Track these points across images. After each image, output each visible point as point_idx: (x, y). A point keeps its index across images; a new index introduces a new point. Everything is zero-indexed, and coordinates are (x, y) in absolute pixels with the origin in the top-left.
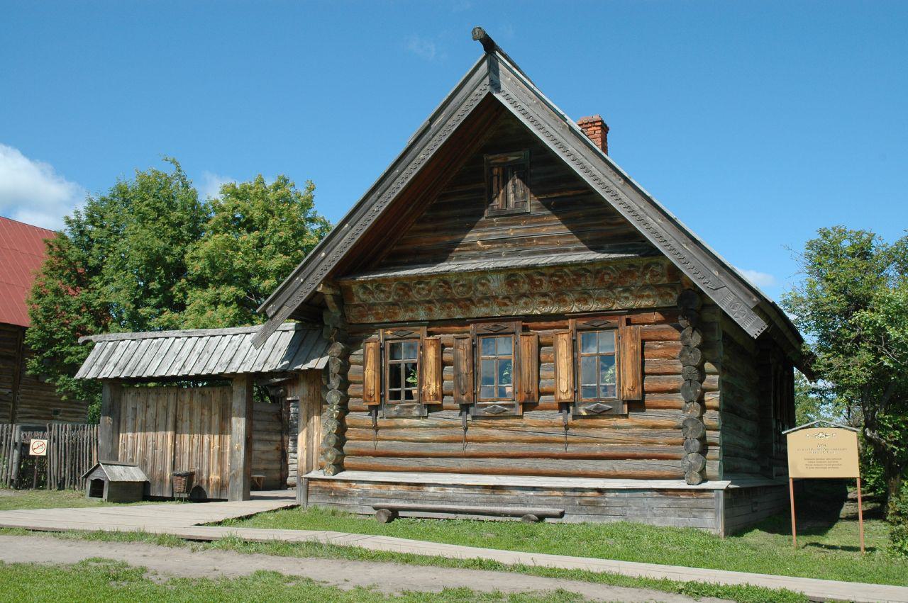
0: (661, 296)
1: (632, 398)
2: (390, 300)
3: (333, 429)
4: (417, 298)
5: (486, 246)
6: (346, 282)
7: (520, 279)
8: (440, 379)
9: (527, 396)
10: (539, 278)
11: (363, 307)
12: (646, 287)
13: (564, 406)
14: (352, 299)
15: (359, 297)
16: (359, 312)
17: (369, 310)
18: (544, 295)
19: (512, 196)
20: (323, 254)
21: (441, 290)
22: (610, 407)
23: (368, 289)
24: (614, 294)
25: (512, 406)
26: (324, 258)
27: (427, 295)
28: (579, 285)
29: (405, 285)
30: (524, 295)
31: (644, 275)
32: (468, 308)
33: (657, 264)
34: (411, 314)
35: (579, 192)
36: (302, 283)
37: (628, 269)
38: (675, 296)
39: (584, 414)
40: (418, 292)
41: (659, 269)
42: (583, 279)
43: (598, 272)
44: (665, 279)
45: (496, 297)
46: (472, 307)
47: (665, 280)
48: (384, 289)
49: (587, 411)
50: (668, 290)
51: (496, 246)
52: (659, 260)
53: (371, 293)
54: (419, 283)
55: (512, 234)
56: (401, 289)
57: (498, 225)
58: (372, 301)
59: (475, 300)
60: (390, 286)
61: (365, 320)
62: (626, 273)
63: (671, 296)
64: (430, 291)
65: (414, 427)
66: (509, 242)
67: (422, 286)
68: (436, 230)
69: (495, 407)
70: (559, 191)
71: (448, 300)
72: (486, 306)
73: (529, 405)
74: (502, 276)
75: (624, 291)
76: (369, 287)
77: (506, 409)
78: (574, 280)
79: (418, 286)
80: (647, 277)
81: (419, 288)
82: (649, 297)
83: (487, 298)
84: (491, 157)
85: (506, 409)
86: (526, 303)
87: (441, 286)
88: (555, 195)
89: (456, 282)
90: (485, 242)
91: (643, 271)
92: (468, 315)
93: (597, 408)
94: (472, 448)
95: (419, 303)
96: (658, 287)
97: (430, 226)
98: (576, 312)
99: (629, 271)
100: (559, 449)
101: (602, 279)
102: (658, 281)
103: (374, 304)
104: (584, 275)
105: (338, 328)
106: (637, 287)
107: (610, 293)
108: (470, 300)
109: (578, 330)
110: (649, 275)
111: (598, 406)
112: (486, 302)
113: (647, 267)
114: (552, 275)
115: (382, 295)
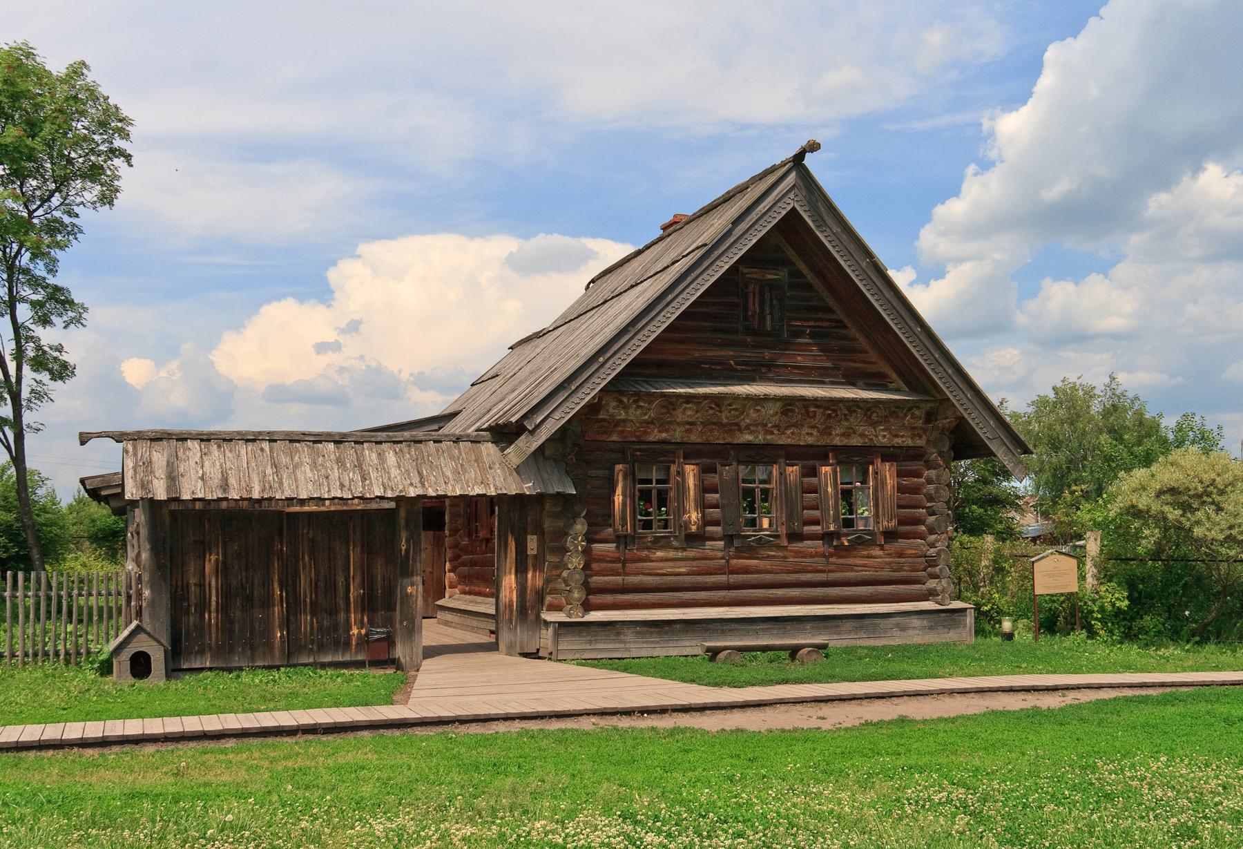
0: (913, 437)
8: (703, 505)
12: (904, 427)
13: (828, 537)
17: (616, 426)
18: (814, 427)
19: (768, 318)
21: (711, 412)
23: (621, 402)
27: (691, 416)
28: (847, 420)
29: (671, 403)
30: (794, 425)
31: (906, 415)
32: (731, 432)
34: (664, 435)
38: (924, 437)
41: (917, 413)
43: (868, 409)
46: (738, 433)
47: (920, 423)
50: (921, 432)
53: (626, 408)
54: (688, 402)
56: (663, 407)
58: (623, 415)
59: (743, 424)
60: (650, 403)
61: (604, 437)
62: (892, 414)
63: (921, 437)
65: (667, 562)
66: (763, 366)
68: (681, 342)
70: (815, 320)
72: (751, 433)
73: (795, 537)
74: (778, 404)
76: (625, 400)
83: (756, 425)
84: (746, 270)
88: (811, 323)
92: (729, 440)
94: (734, 578)
95: (679, 424)
96: (913, 428)
101: (870, 417)
103: (624, 421)
108: (737, 425)
114: (828, 408)
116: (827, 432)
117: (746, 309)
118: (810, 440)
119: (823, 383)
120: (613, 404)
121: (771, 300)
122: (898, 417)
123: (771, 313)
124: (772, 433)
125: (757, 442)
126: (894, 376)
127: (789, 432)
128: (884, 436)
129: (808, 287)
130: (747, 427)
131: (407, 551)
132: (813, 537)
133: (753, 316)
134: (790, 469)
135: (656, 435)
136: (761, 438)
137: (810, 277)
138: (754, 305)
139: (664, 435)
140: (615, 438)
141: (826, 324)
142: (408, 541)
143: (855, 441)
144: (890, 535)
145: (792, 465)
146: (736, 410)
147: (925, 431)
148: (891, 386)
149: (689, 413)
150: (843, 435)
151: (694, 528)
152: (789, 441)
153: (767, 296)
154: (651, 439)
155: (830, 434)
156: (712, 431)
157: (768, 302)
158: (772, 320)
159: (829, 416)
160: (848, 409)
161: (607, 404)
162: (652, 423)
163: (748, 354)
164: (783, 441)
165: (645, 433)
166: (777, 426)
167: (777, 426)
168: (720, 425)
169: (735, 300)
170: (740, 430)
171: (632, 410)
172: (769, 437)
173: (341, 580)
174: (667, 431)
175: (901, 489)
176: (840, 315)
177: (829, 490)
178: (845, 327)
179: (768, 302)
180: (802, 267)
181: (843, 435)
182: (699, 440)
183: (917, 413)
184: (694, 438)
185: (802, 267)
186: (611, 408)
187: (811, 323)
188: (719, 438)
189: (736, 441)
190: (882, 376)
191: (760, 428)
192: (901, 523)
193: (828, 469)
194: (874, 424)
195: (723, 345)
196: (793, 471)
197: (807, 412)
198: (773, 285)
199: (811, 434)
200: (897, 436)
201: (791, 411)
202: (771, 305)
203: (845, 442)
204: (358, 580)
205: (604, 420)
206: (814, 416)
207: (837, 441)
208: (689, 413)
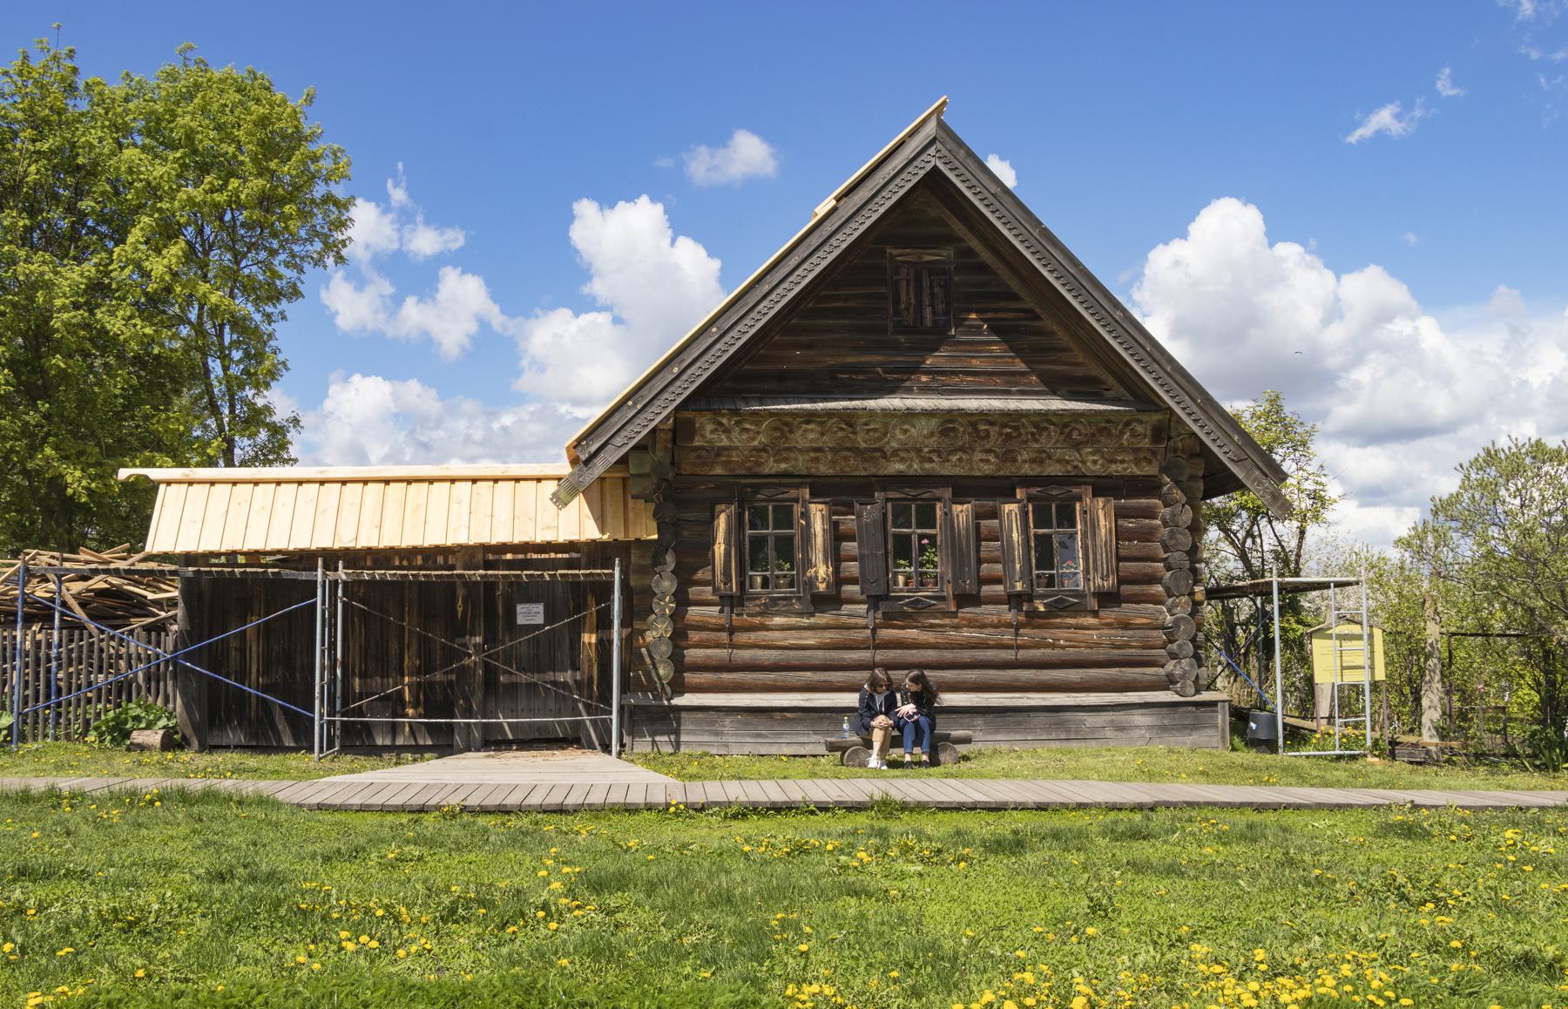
2: (756, 443)
4: (802, 444)
6: (690, 415)
12: (1122, 449)
13: (1014, 600)
14: (691, 439)
15: (703, 436)
16: (699, 457)
19: (928, 310)
21: (840, 434)
23: (720, 424)
25: (942, 599)
28: (1037, 441)
29: (786, 424)
30: (961, 449)
31: (1122, 433)
34: (783, 466)
40: (804, 436)
41: (1139, 429)
43: (1066, 425)
45: (919, 451)
47: (1146, 443)
50: (1149, 456)
53: (727, 431)
54: (808, 422)
56: (776, 429)
58: (725, 442)
60: (758, 424)
61: (705, 470)
62: (1102, 431)
63: (1150, 462)
64: (822, 434)
68: (810, 346)
70: (996, 311)
71: (848, 449)
72: (902, 460)
74: (934, 422)
75: (1093, 454)
76: (724, 421)
78: (1033, 434)
79: (805, 426)
82: (1122, 462)
83: (907, 451)
84: (895, 252)
86: (960, 460)
89: (866, 424)
92: (872, 471)
97: (803, 339)
100: (1008, 655)
101: (1069, 436)
112: (902, 454)
113: (1127, 424)
114: (1005, 426)
115: (745, 436)
116: (1008, 457)
117: (897, 301)
118: (987, 469)
119: (1008, 393)
120: (710, 427)
121: (931, 288)
122: (1110, 435)
123: (932, 305)
124: (931, 461)
125: (911, 472)
126: (1111, 381)
127: (954, 458)
128: (1095, 462)
129: (983, 268)
130: (895, 452)
131: (465, 613)
132: (994, 600)
133: (907, 309)
134: (957, 508)
135: (772, 466)
136: (916, 467)
137: (985, 256)
138: (906, 296)
139: (783, 466)
140: (719, 471)
141: (1012, 315)
142: (465, 602)
143: (1053, 469)
144: (1108, 599)
145: (962, 503)
146: (875, 430)
148: (1108, 394)
149: (811, 436)
150: (1033, 461)
151: (822, 587)
152: (958, 471)
153: (926, 283)
154: (766, 471)
155: (1015, 460)
156: (846, 459)
157: (926, 291)
158: (934, 313)
159: (1008, 435)
160: (1036, 425)
161: (702, 427)
162: (764, 450)
164: (946, 470)
165: (759, 464)
166: (938, 452)
167: (938, 452)
168: (858, 452)
169: (883, 290)
170: (885, 456)
171: (735, 434)
172: (927, 466)
173: (394, 646)
174: (786, 460)
175: (1121, 534)
176: (1029, 303)
177: (1015, 535)
178: (1038, 318)
179: (926, 291)
180: (974, 244)
181: (1033, 461)
182: (831, 472)
183: (1139, 429)
184: (823, 469)
185: (974, 244)
186: (708, 432)
188: (857, 468)
189: (882, 472)
190: (1094, 381)
191: (913, 454)
192: (1121, 581)
193: (1014, 507)
194: (1077, 446)
195: (866, 350)
196: (962, 512)
197: (977, 431)
198: (934, 269)
199: (988, 461)
200: (1113, 461)
201: (953, 430)
202: (932, 295)
204: (414, 647)
205: (702, 448)
206: (988, 436)
207: (1027, 470)
208: (811, 436)
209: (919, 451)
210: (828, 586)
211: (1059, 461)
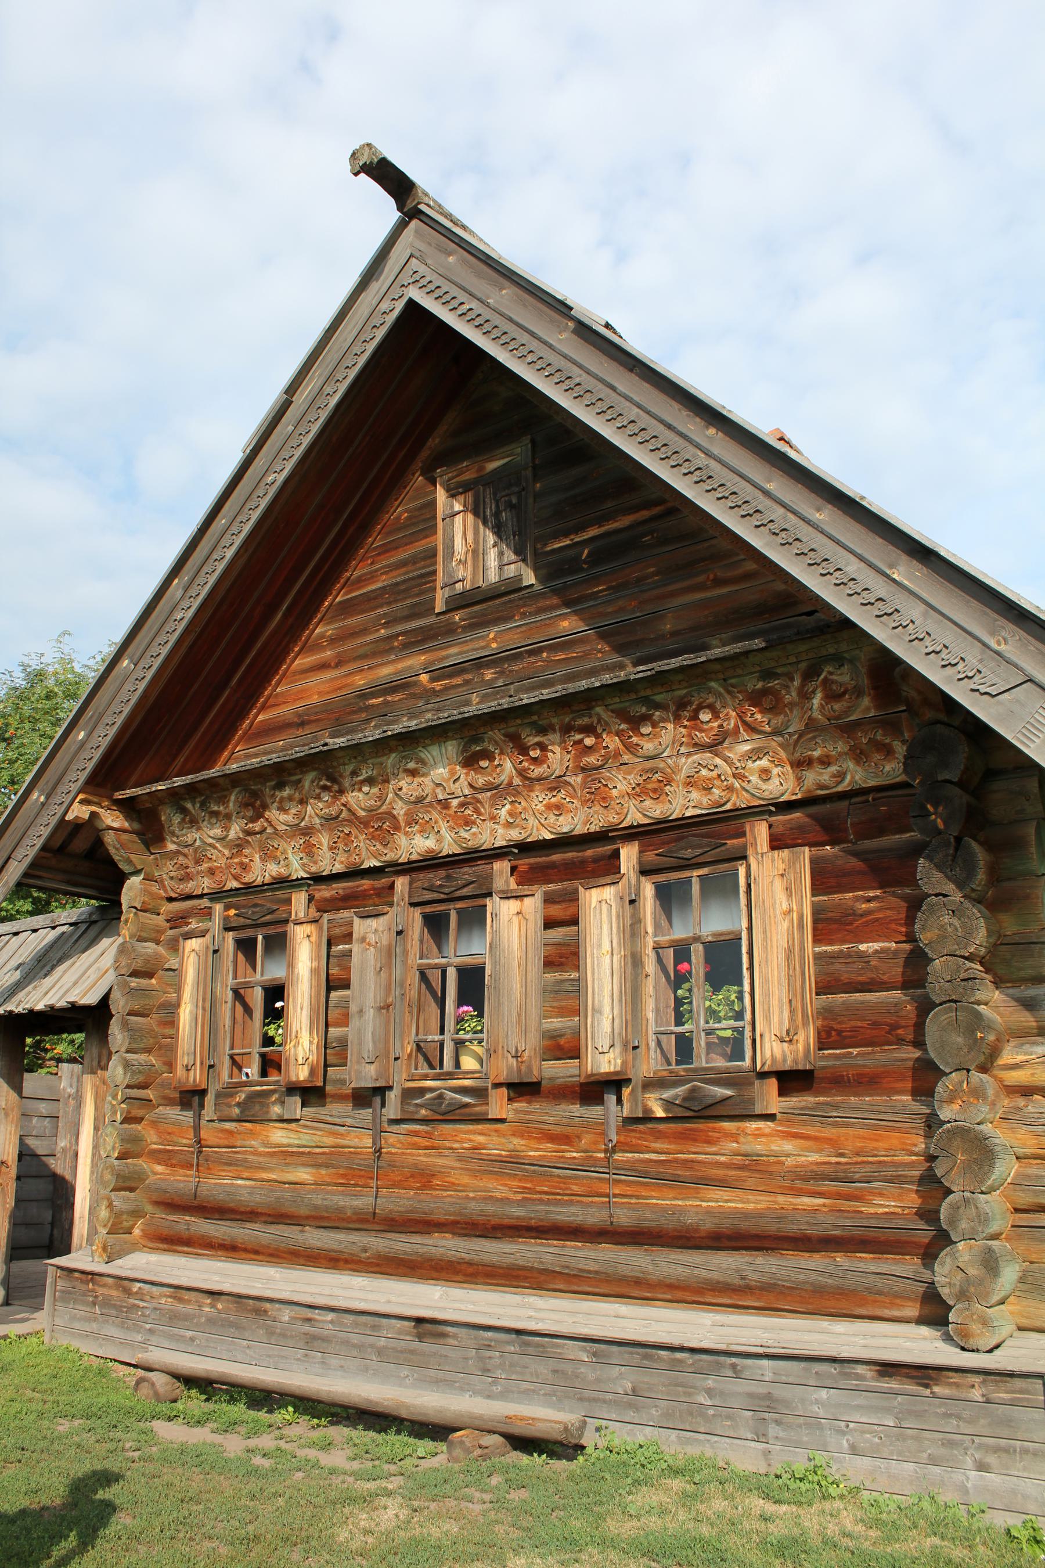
0: (859, 755)
1: (788, 1065)
3: (114, 1148)
5: (438, 686)
7: (491, 748)
9: (513, 1062)
10: (537, 739)
11: (185, 855)
17: (198, 862)
18: (556, 784)
20: (82, 735)
22: (729, 1092)
24: (726, 760)
26: (83, 743)
31: (805, 696)
33: (838, 660)
35: (645, 514)
36: (43, 804)
37: (760, 685)
38: (900, 749)
39: (660, 1113)
40: (281, 809)
41: (843, 677)
42: (646, 730)
44: (866, 701)
45: (445, 804)
47: (865, 707)
48: (216, 808)
49: (668, 1104)
51: (459, 681)
52: (844, 647)
54: (280, 786)
55: (494, 645)
57: (464, 627)
63: (888, 752)
67: (286, 792)
69: (441, 1097)
77: (467, 1100)
79: (279, 794)
80: (816, 701)
81: (282, 799)
82: (825, 761)
85: (467, 1100)
87: (325, 788)
90: (437, 674)
91: (803, 685)
92: (390, 856)
93: (692, 1096)
98: (639, 826)
99: (765, 692)
102: (847, 712)
104: (645, 718)
105: (135, 908)
106: (791, 734)
107: (718, 761)
109: (645, 871)
110: (819, 695)
111: (694, 1090)
124: (468, 823)
140: (206, 884)
147: (891, 726)
150: (640, 792)
163: (454, 653)
181: (640, 792)
187: (592, 532)
203: (657, 810)
207: (634, 815)
209: (445, 804)
210: (312, 1072)
211: (690, 782)
